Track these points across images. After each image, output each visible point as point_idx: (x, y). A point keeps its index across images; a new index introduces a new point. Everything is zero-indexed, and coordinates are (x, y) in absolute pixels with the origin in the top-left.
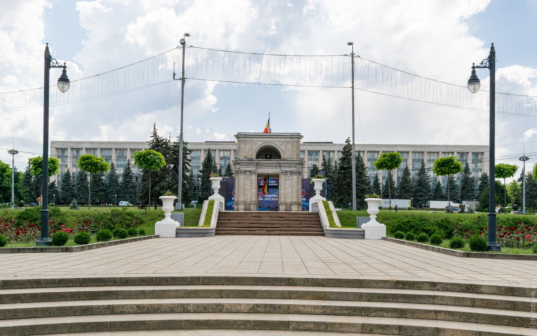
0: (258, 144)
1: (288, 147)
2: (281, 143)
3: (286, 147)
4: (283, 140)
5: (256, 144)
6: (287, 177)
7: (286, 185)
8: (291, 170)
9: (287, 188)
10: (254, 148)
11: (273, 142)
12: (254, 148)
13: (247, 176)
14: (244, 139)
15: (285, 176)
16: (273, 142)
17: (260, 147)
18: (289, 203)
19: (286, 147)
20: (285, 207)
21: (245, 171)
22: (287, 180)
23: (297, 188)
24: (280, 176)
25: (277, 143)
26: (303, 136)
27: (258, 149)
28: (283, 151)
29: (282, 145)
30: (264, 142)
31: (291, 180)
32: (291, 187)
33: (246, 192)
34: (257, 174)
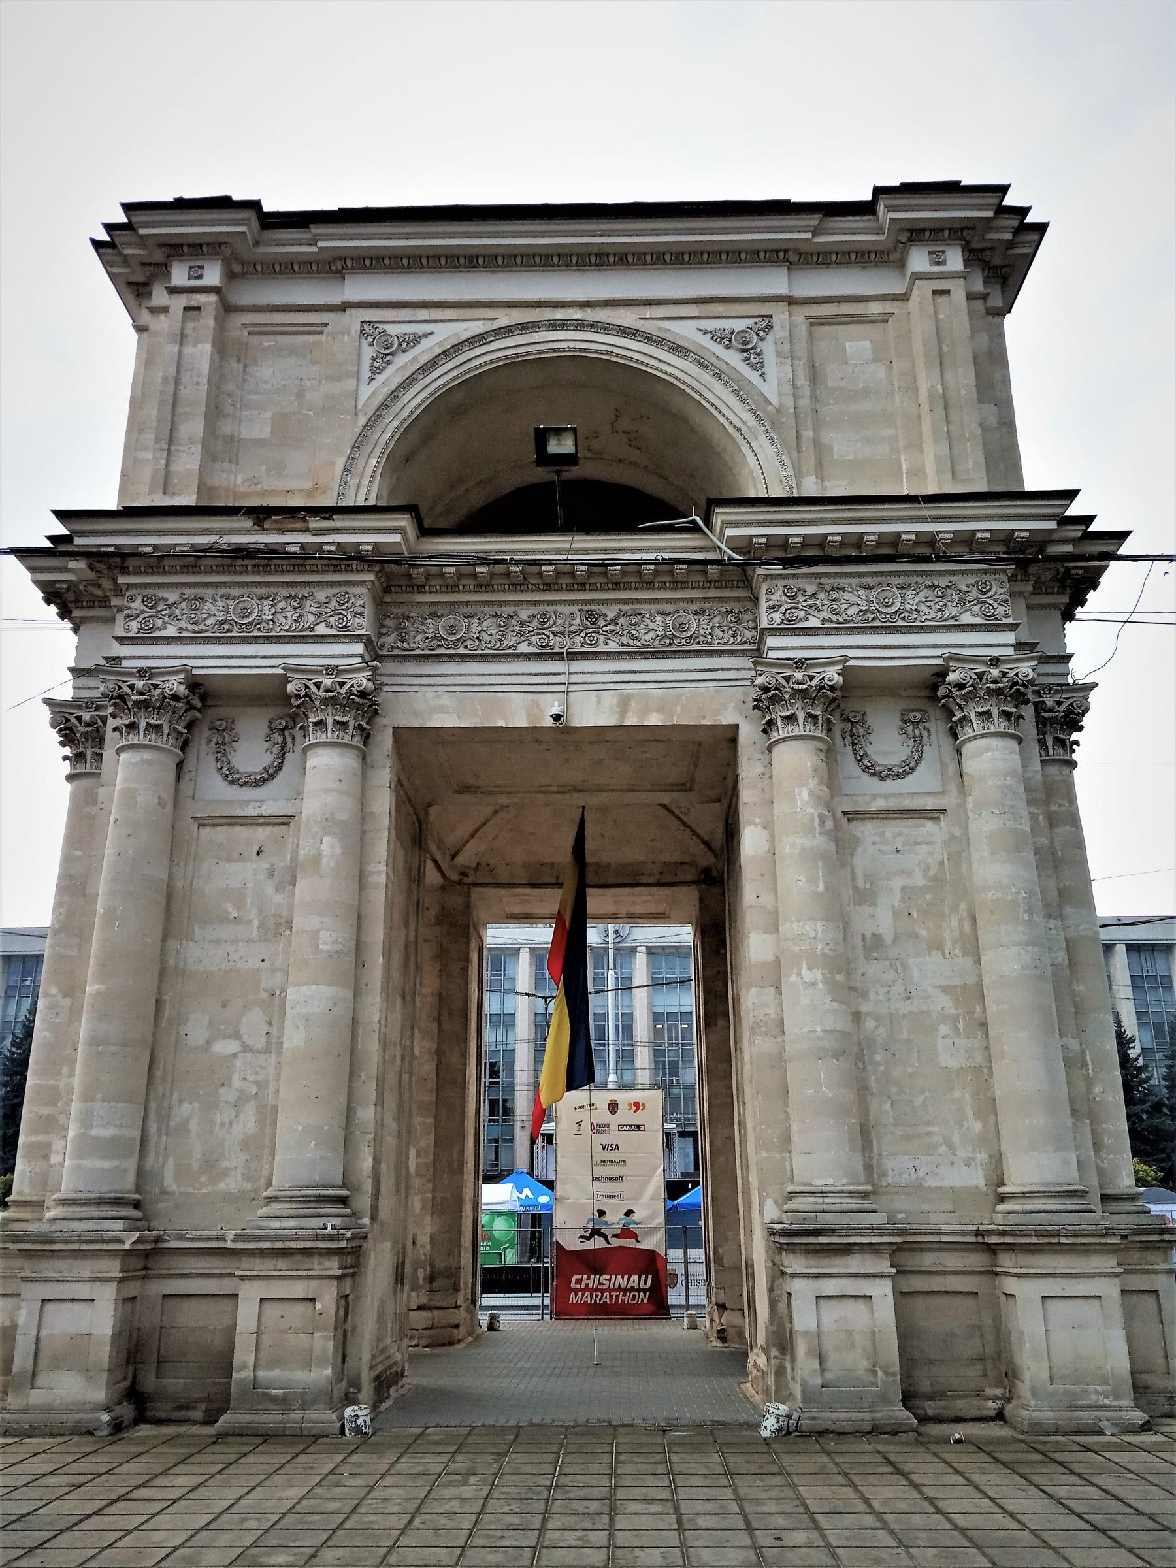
0: (416, 340)
1: (833, 375)
2: (739, 325)
3: (815, 374)
4: (775, 282)
5: (388, 351)
6: (874, 785)
7: (865, 897)
8: (930, 658)
9: (873, 946)
10: (365, 392)
11: (627, 318)
12: (365, 392)
13: (234, 779)
14: (213, 276)
15: (830, 755)
16: (627, 318)
17: (444, 376)
18: (941, 1216)
19: (815, 374)
20: (883, 1291)
21: (195, 684)
22: (867, 830)
23: (1061, 956)
24: (749, 769)
25: (687, 331)
26: (1042, 228)
27: (414, 401)
28: (770, 421)
29: (747, 350)
30: (505, 318)
31: (934, 815)
32: (952, 926)
33: (196, 1031)
34: (385, 742)
